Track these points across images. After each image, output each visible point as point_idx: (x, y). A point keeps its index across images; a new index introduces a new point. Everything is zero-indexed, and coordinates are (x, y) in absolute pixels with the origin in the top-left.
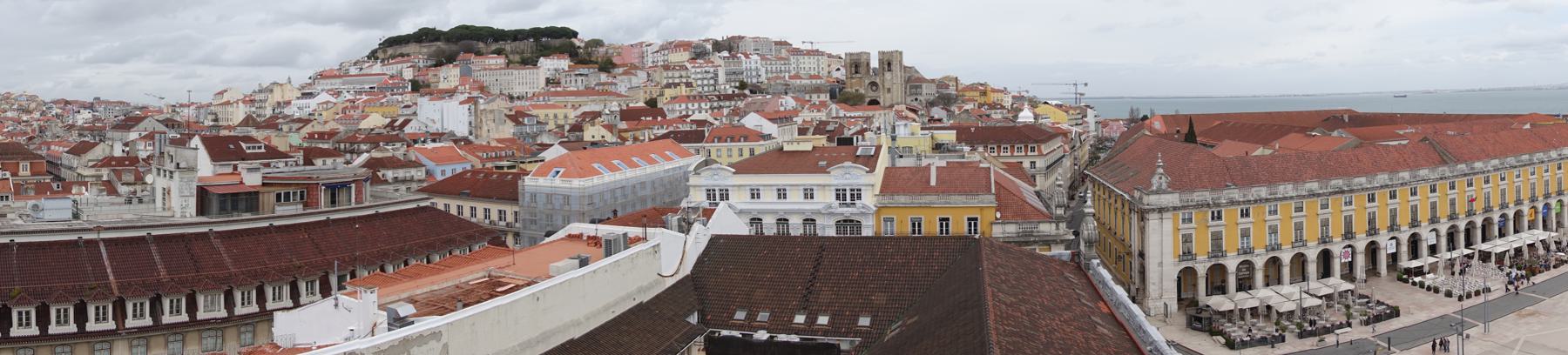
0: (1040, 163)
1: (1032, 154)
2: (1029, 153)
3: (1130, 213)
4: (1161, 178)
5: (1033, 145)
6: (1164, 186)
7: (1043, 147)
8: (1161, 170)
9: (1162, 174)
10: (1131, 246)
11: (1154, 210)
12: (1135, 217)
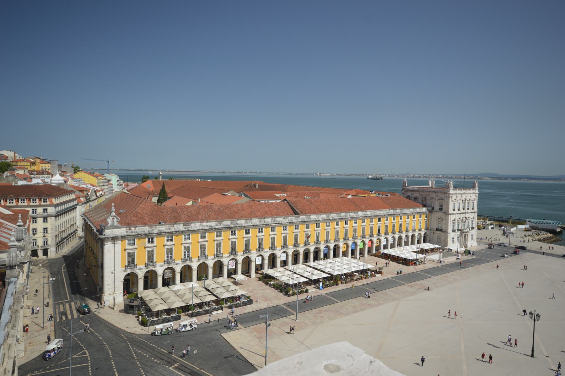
0: (51, 210)
1: (45, 203)
2: (42, 203)
3: (98, 240)
4: (113, 219)
5: (45, 198)
6: (116, 223)
7: (53, 200)
8: (113, 214)
9: (114, 216)
10: (98, 261)
11: (108, 238)
12: (100, 242)
